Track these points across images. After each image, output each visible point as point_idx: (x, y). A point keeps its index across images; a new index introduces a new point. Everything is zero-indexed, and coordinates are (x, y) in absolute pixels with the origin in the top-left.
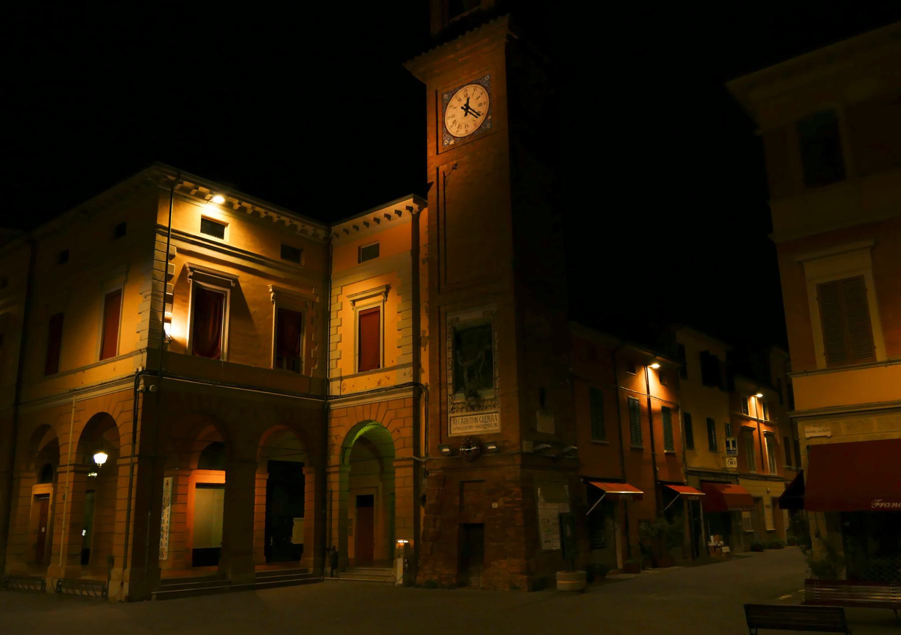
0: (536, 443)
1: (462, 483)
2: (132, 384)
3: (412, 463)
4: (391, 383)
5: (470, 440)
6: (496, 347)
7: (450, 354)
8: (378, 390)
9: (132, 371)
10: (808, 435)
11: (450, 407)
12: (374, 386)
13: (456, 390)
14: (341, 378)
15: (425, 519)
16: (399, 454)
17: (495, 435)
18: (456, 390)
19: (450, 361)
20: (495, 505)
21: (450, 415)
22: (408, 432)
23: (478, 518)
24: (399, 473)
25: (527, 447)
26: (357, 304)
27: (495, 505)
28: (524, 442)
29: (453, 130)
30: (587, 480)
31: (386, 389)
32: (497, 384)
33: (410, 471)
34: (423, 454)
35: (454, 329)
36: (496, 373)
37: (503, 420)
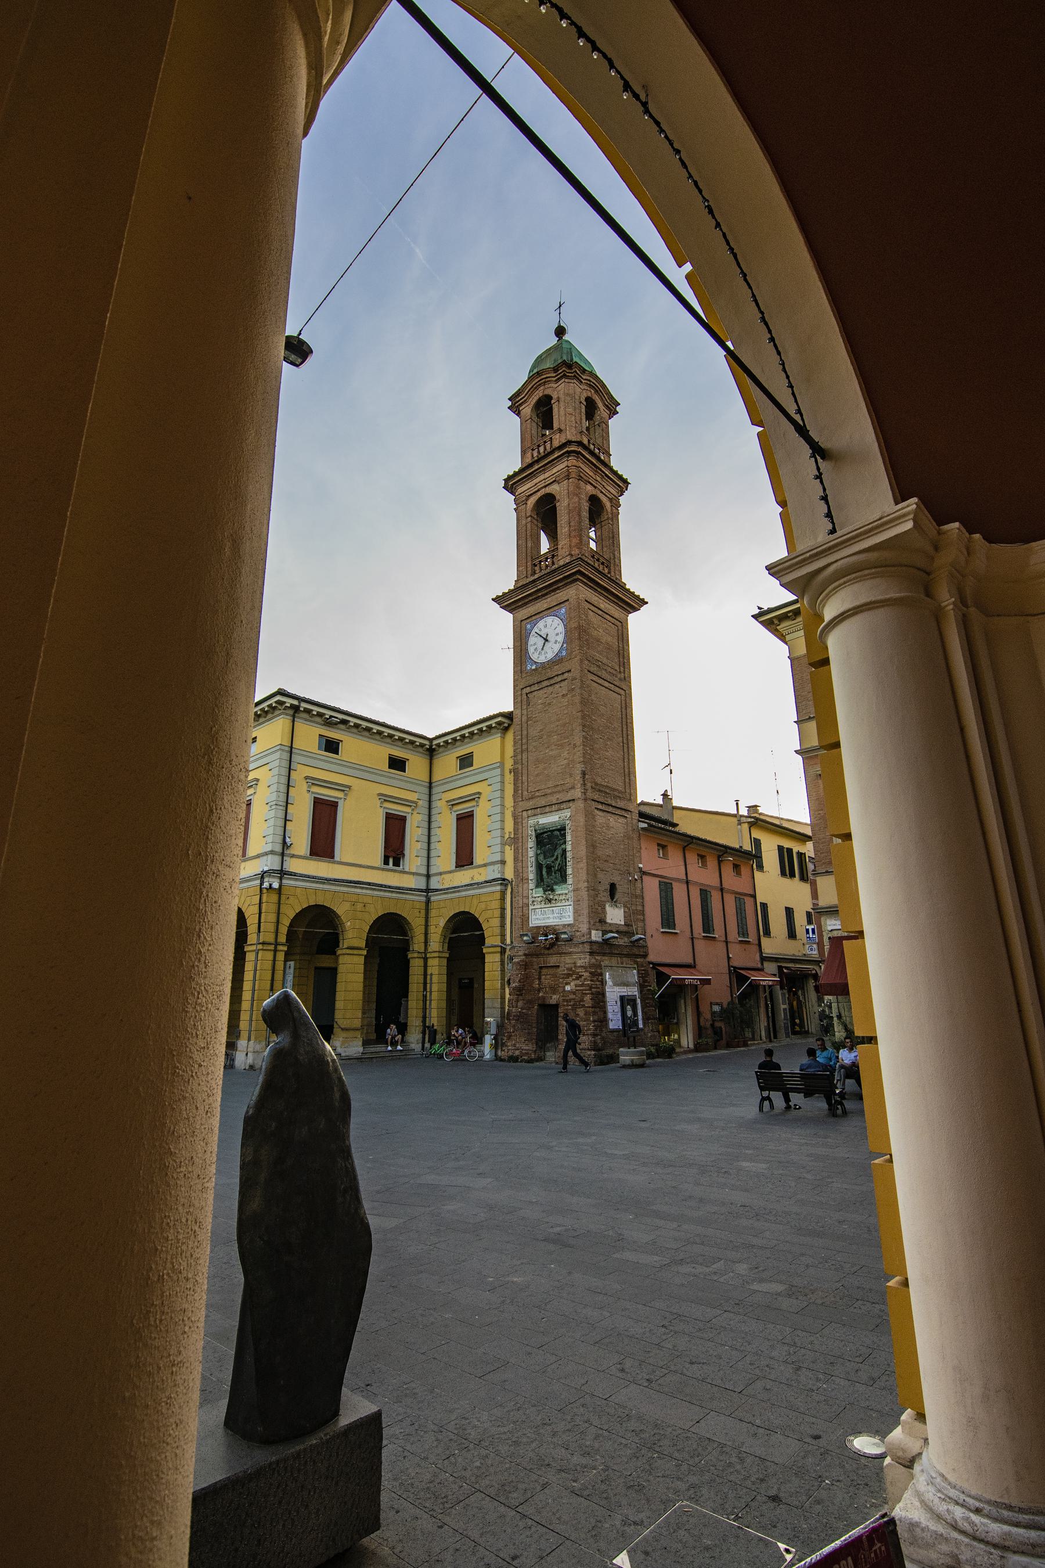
0: (604, 932)
1: (541, 968)
2: (258, 882)
3: (499, 949)
4: (482, 879)
5: (546, 930)
6: (569, 848)
7: (531, 853)
8: (471, 885)
9: (259, 871)
10: (830, 928)
11: (531, 900)
12: (468, 881)
13: (537, 887)
14: (441, 874)
15: (509, 1000)
16: (488, 942)
17: (569, 925)
18: (537, 887)
19: (533, 859)
20: (568, 988)
21: (531, 907)
22: (496, 922)
23: (554, 999)
24: (488, 958)
25: (596, 936)
26: (456, 808)
27: (568, 988)
28: (593, 932)
29: (535, 657)
30: (655, 965)
31: (478, 884)
32: (570, 880)
33: (497, 957)
34: (508, 941)
36: (569, 871)
37: (576, 912)
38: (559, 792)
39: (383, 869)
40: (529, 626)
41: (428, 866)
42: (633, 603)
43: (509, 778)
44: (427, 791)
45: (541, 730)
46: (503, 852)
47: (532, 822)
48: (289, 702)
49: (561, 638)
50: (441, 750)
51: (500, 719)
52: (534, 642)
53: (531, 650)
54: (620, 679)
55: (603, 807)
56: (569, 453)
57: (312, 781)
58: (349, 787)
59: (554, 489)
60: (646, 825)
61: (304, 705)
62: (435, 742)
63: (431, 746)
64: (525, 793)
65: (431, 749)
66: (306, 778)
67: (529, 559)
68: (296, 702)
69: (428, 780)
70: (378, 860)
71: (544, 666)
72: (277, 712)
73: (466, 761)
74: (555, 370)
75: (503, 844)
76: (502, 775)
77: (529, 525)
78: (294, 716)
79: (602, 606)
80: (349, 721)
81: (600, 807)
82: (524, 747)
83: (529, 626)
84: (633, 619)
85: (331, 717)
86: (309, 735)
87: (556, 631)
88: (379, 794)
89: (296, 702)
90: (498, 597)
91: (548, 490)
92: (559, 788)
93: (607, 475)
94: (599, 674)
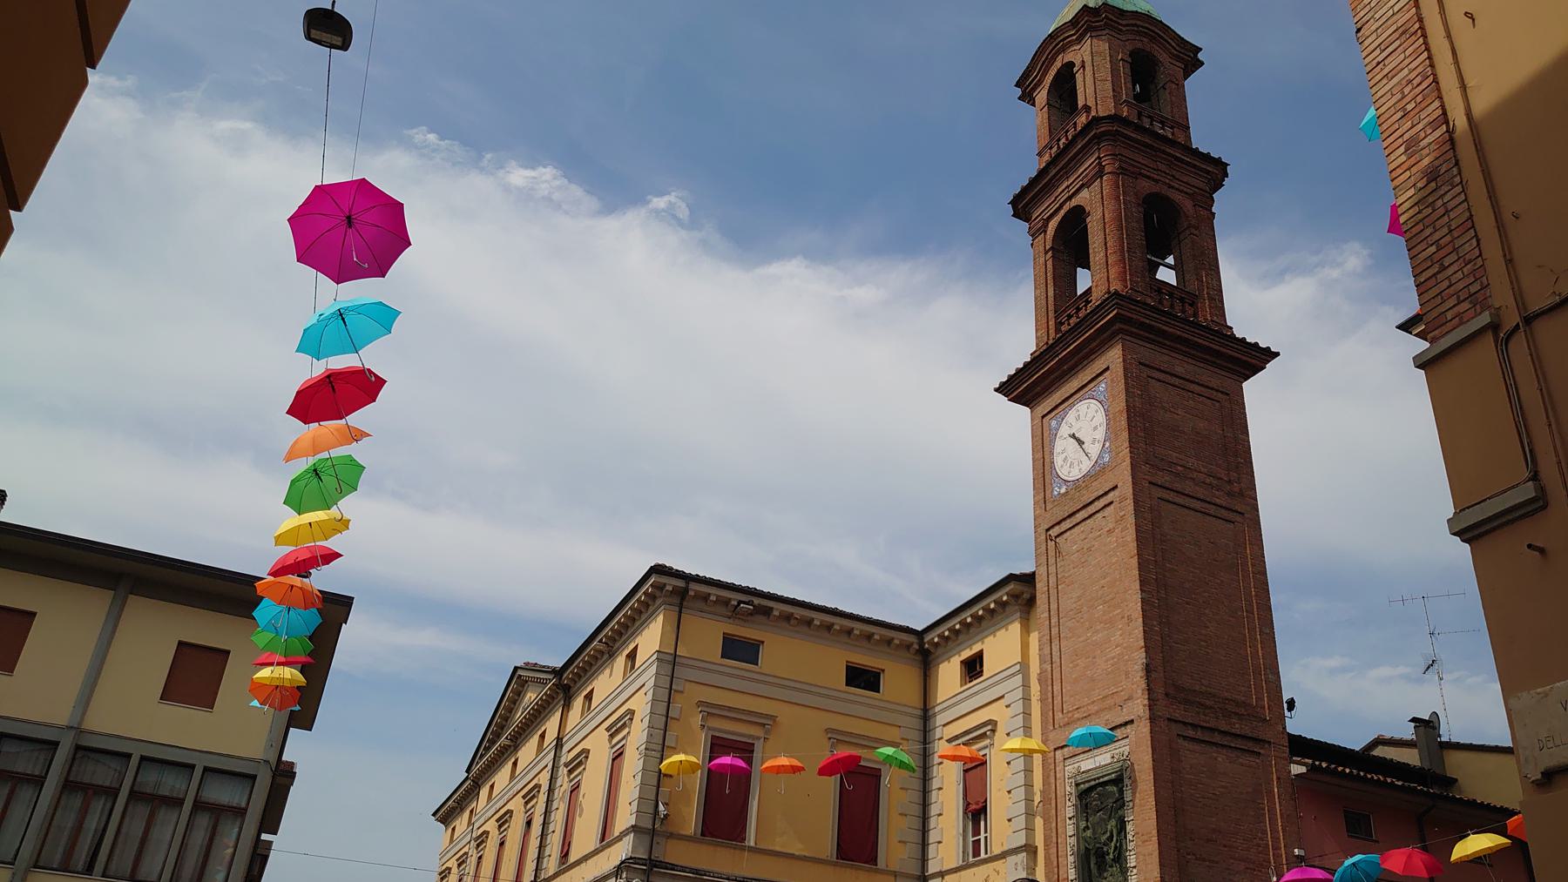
7: (1070, 830)
35: (1077, 785)
38: (1110, 708)
39: (835, 864)
40: (1054, 423)
41: (924, 860)
42: (1256, 358)
43: (1035, 688)
44: (917, 723)
45: (1079, 598)
46: (1030, 829)
47: (1070, 769)
48: (672, 583)
49: (1100, 434)
50: (940, 651)
51: (1011, 587)
52: (1063, 448)
53: (1058, 461)
54: (1230, 494)
55: (1199, 734)
56: (1098, 138)
57: (710, 711)
58: (773, 718)
59: (1084, 198)
60: (1303, 769)
61: (694, 586)
62: (927, 638)
63: (921, 644)
64: (1059, 715)
65: (922, 649)
66: (700, 704)
67: (1051, 314)
68: (680, 583)
69: (918, 703)
70: (826, 843)
71: (1078, 485)
72: (658, 602)
73: (973, 667)
74: (1074, 22)
75: (1030, 815)
76: (1026, 686)
77: (1050, 264)
78: (681, 606)
79: (1179, 370)
80: (771, 609)
81: (1191, 733)
82: (1055, 631)
83: (1054, 423)
84: (1252, 388)
85: (740, 602)
86: (706, 635)
87: (1094, 423)
88: (828, 731)
89: (680, 583)
90: (1003, 385)
91: (1074, 202)
92: (1110, 702)
93: (1177, 159)
94: (1178, 486)
